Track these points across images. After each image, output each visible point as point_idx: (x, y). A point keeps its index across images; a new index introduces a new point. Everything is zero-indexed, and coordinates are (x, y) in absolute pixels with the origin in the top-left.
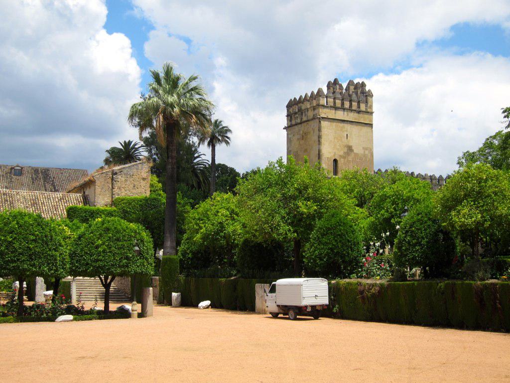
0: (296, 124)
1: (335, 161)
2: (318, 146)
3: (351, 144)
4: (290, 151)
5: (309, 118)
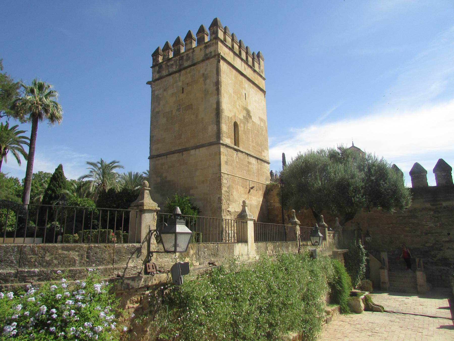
0: (170, 74)
1: (236, 125)
2: (216, 97)
3: (250, 108)
4: (158, 113)
5: (195, 61)
